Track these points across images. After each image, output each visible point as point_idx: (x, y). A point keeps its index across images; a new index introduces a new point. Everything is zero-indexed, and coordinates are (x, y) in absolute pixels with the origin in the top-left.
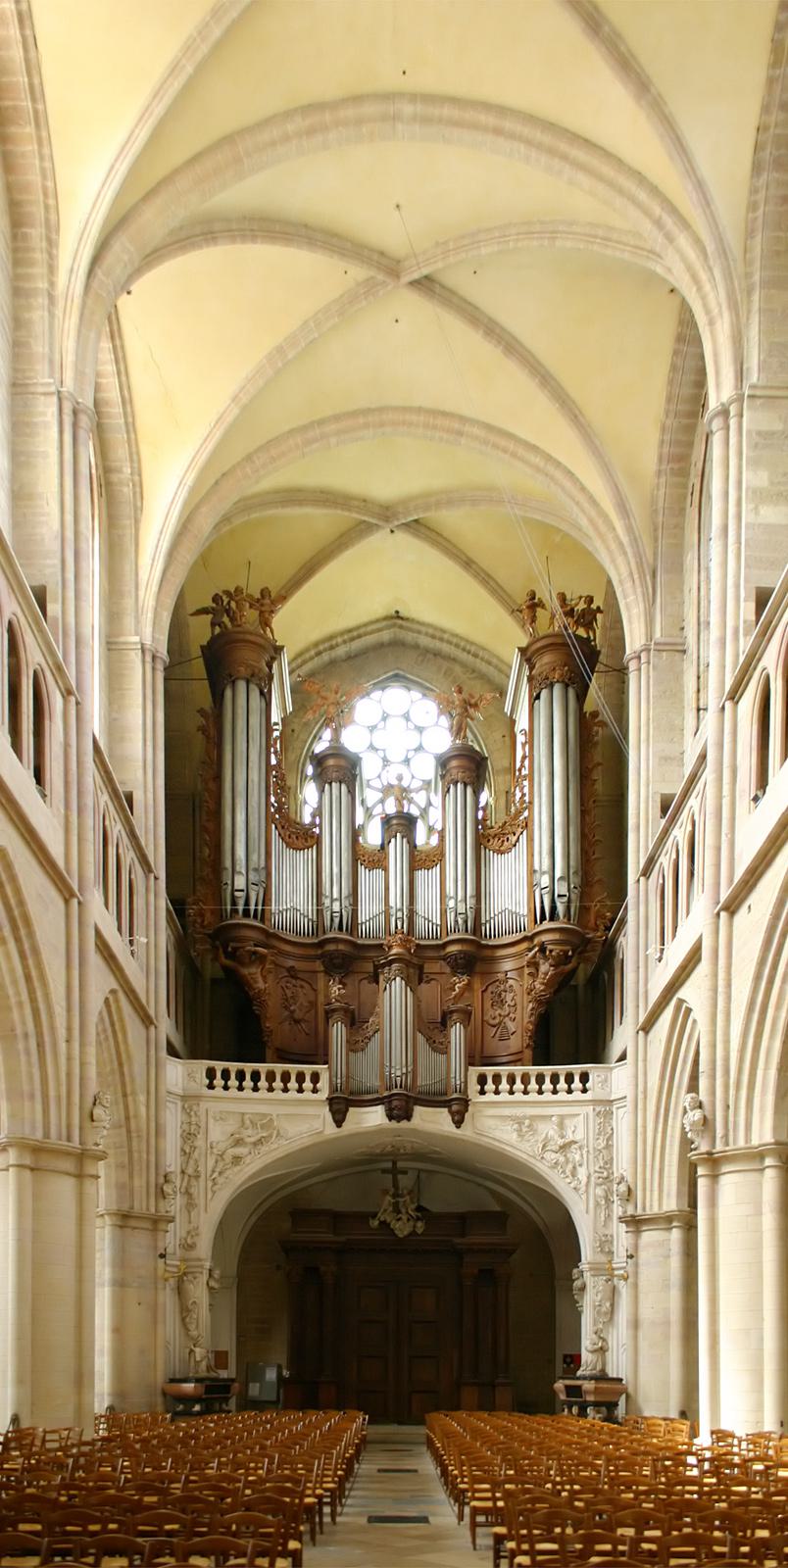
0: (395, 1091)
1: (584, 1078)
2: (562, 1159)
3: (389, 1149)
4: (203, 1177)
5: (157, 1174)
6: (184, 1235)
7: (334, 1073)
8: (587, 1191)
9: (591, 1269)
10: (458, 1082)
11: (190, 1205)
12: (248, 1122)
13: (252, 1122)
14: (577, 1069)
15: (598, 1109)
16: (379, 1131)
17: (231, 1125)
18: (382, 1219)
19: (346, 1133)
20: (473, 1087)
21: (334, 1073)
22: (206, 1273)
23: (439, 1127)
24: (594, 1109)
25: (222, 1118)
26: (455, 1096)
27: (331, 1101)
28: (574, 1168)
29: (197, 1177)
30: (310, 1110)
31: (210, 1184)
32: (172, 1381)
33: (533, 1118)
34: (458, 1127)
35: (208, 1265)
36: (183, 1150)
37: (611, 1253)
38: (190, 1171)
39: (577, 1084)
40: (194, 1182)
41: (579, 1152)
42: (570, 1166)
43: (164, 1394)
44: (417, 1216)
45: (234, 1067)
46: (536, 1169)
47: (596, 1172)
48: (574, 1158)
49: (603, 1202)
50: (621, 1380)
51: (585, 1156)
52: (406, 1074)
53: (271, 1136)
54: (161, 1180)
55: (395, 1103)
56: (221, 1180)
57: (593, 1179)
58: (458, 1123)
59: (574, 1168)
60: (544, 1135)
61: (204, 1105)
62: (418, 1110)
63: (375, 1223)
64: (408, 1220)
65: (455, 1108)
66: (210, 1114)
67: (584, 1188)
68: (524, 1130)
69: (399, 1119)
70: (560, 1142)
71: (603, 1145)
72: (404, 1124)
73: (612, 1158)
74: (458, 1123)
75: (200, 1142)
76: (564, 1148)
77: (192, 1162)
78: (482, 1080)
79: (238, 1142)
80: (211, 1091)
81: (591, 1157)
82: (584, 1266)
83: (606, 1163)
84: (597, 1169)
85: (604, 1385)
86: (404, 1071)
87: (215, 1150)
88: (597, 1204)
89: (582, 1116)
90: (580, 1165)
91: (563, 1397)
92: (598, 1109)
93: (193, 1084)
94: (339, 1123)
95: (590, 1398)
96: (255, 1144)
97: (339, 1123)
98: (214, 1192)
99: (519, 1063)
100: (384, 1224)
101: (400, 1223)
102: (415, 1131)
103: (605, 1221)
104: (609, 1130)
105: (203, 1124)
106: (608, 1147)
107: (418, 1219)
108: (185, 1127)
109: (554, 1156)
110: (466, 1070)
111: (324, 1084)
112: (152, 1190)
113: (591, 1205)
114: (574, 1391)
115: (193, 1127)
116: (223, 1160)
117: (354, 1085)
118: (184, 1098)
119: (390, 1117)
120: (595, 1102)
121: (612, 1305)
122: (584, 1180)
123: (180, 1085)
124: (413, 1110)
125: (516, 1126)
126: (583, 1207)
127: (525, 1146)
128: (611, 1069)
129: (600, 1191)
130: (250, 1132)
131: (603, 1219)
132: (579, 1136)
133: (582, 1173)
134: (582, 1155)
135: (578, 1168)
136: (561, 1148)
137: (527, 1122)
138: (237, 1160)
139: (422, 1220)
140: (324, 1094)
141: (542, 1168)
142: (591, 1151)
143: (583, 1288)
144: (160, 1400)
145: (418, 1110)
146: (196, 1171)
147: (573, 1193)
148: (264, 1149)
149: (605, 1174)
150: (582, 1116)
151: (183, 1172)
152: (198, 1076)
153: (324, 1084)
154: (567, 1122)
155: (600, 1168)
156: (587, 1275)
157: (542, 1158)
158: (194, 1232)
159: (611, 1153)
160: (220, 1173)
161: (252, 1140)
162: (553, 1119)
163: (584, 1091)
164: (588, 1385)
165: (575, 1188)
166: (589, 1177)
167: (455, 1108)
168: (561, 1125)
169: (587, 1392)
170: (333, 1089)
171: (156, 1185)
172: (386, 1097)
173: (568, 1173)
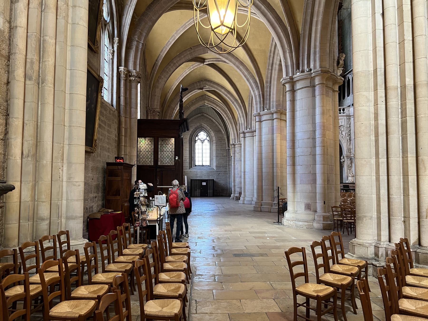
1: (344, 110)
9: (346, 156)
15: (347, 118)
37: (351, 152)
39: (342, 111)
42: (341, 131)
47: (347, 133)
49: (349, 140)
57: (346, 134)
67: (344, 137)
73: (351, 130)
81: (346, 129)
83: (349, 131)
84: (347, 132)
88: (347, 140)
89: (343, 120)
90: (343, 131)
92: (347, 118)
104: (350, 123)
106: (350, 127)
113: (346, 141)
120: (346, 116)
121: (351, 165)
126: (344, 142)
128: (350, 108)
129: (348, 138)
131: (349, 144)
132: (343, 124)
134: (344, 129)
135: (343, 132)
149: (349, 133)
150: (343, 120)
156: (345, 158)
159: (350, 128)
163: (344, 113)
166: (345, 134)
173: (341, 133)
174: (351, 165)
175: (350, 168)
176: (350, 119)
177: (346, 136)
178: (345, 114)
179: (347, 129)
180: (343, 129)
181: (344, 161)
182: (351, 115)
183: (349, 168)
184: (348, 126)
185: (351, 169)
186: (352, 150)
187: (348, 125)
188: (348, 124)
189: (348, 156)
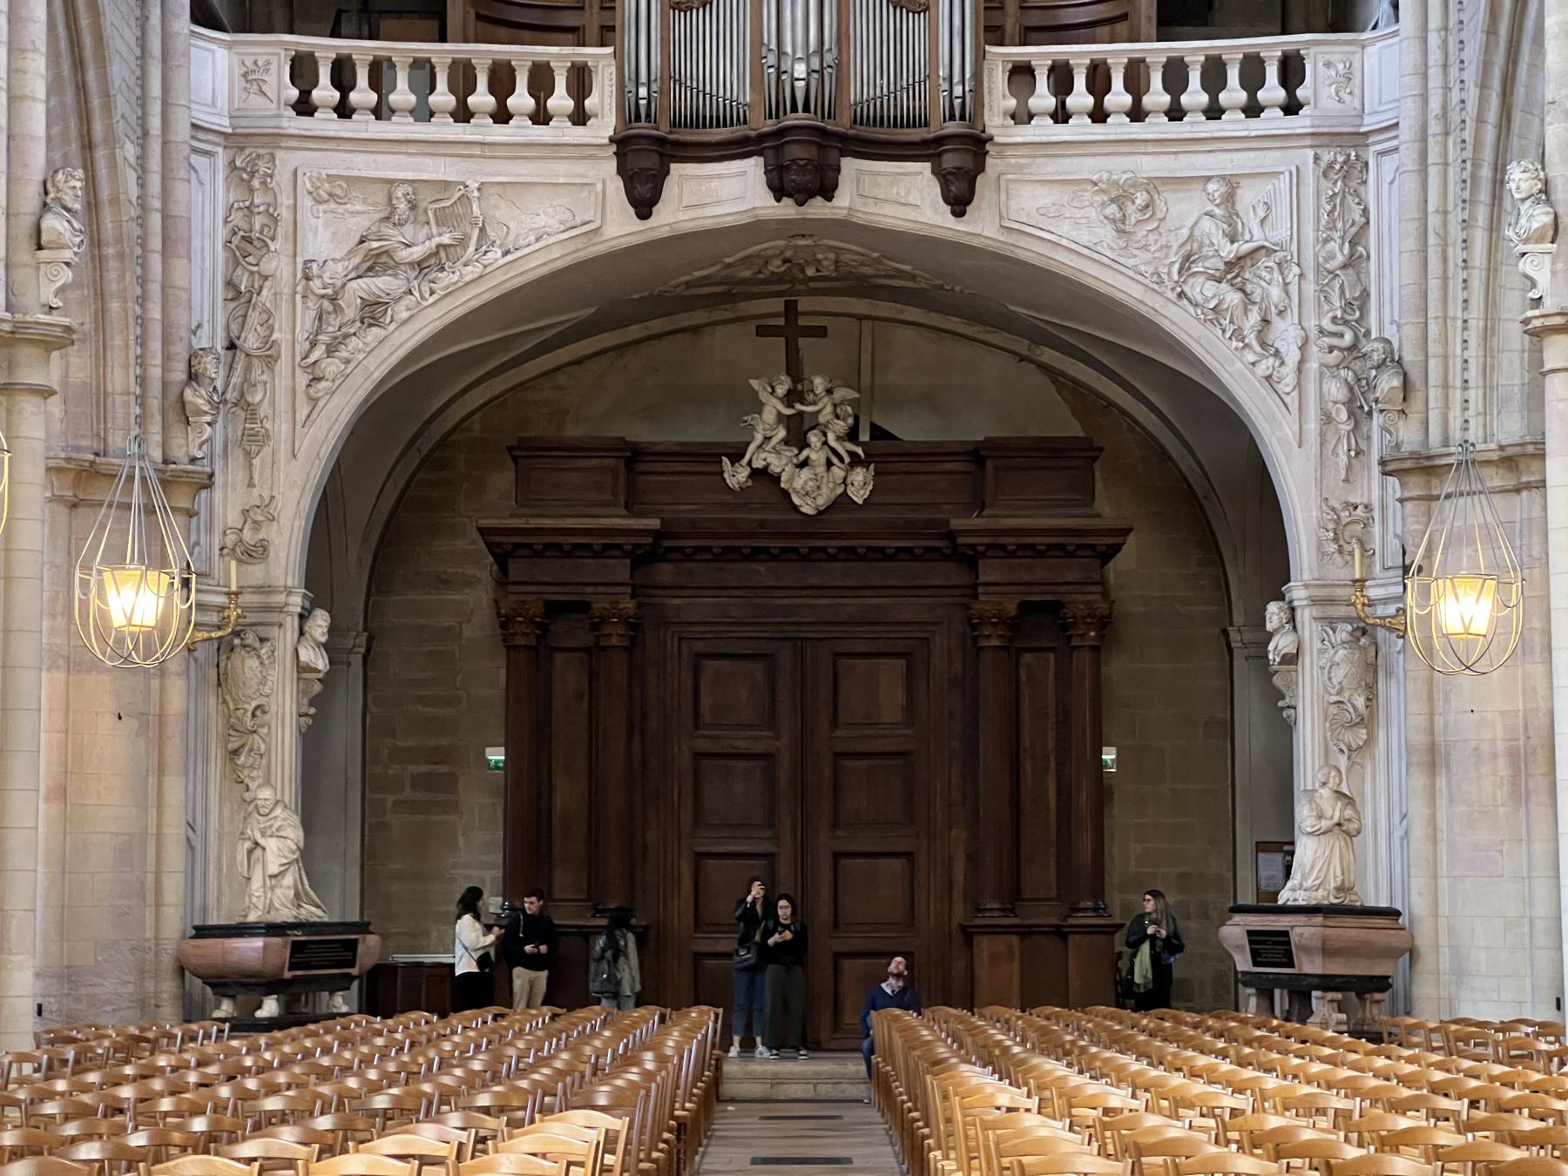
0: (791, 120)
1: (1292, 71)
2: (1233, 298)
3: (776, 266)
4: (283, 365)
5: (167, 358)
6: (234, 518)
7: (628, 71)
8: (1299, 385)
9: (1315, 602)
10: (958, 91)
11: (253, 441)
12: (402, 206)
13: (413, 207)
14: (1271, 46)
15: (1327, 156)
16: (755, 229)
17: (360, 216)
18: (759, 464)
19: (665, 232)
20: (999, 98)
21: (628, 71)
22: (292, 623)
23: (911, 214)
24: (1317, 158)
25: (337, 190)
26: (953, 127)
27: (623, 145)
28: (1266, 321)
29: (270, 360)
30: (562, 170)
31: (302, 379)
32: (203, 932)
33: (1154, 185)
34: (959, 213)
35: (296, 602)
36: (230, 284)
38: (251, 342)
39: (1272, 91)
40: (258, 373)
41: (1277, 275)
42: (1254, 317)
43: (181, 970)
44: (851, 454)
45: (362, 50)
46: (1166, 325)
47: (1322, 331)
48: (1266, 296)
49: (1344, 415)
50: (1398, 914)
51: (1294, 289)
52: (821, 72)
53: (462, 242)
54: (179, 375)
55: (795, 152)
56: (331, 367)
57: (1313, 350)
58: (959, 203)
59: (1266, 321)
60: (1185, 232)
61: (287, 161)
62: (851, 167)
63: (737, 476)
64: (829, 464)
65: (950, 161)
66: (305, 183)
68: (1133, 215)
69: (802, 195)
70: (1229, 251)
71: (1340, 259)
72: (817, 208)
73: (1365, 294)
74: (959, 203)
75: (278, 264)
76: (1235, 265)
77: (254, 318)
78: (1021, 73)
79: (376, 263)
80: (305, 121)
81: (1310, 287)
82: (1297, 592)
84: (1327, 324)
85: (1347, 931)
86: (815, 64)
87: (316, 285)
88: (1327, 419)
91: (1243, 963)
92: (1327, 156)
93: (257, 101)
94: (644, 206)
95: (1310, 965)
96: (421, 266)
97: (644, 206)
98: (314, 401)
99: (1121, 27)
100: (761, 475)
101: (805, 473)
102: (844, 227)
103: (1349, 469)
104: (1357, 214)
105: (285, 213)
106: (1354, 262)
107: (856, 461)
108: (237, 218)
109: (1210, 288)
110: (980, 56)
111: (602, 100)
112: (154, 403)
113: (1312, 426)
114: (1272, 947)
115: (258, 222)
116: (338, 310)
117: (684, 102)
118: (235, 140)
119: (779, 191)
122: (1292, 356)
123: (223, 103)
124: (838, 171)
125: (1112, 210)
126: (1289, 430)
127: (1140, 260)
129: (1335, 390)
130: (408, 230)
132: (1280, 231)
133: (1286, 335)
135: (1278, 324)
136: (1230, 265)
137: (1141, 198)
138: (373, 312)
139: (864, 464)
140: (604, 125)
141: (1181, 323)
142: (1311, 276)
143: (1291, 659)
144: (169, 986)
145: (851, 167)
146: (268, 343)
147: (1264, 390)
148: (446, 279)
149: (1348, 338)
151: (232, 346)
152: (271, 78)
153: (602, 100)
154: (1248, 196)
155: (1334, 320)
156: (1304, 616)
157: (1182, 295)
158: (259, 513)
160: (330, 352)
161: (417, 253)
162: (1212, 186)
164: (1302, 931)
165: (1268, 378)
166: (1303, 347)
167: (950, 161)
168: (1229, 199)
169: (1305, 949)
170: (630, 113)
171: (165, 385)
172: (763, 137)
173: (1251, 338)
174: (1360, 702)
175: (1363, 734)
176: (1352, 172)
177: (1313, 366)
178: (1298, 123)
179: (1324, 293)
180: (1275, 293)
181: (1291, 659)
182: (1370, 123)
183: (1348, 736)
184: (1331, 257)
185: (1370, 742)
186: (1376, 529)
187: (1334, 246)
188: (1332, 227)
189: (1331, 601)
